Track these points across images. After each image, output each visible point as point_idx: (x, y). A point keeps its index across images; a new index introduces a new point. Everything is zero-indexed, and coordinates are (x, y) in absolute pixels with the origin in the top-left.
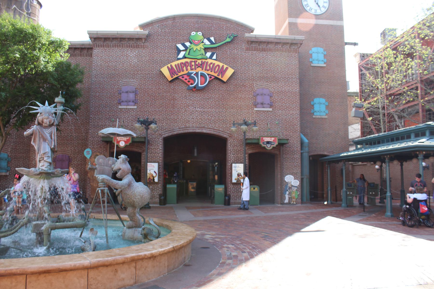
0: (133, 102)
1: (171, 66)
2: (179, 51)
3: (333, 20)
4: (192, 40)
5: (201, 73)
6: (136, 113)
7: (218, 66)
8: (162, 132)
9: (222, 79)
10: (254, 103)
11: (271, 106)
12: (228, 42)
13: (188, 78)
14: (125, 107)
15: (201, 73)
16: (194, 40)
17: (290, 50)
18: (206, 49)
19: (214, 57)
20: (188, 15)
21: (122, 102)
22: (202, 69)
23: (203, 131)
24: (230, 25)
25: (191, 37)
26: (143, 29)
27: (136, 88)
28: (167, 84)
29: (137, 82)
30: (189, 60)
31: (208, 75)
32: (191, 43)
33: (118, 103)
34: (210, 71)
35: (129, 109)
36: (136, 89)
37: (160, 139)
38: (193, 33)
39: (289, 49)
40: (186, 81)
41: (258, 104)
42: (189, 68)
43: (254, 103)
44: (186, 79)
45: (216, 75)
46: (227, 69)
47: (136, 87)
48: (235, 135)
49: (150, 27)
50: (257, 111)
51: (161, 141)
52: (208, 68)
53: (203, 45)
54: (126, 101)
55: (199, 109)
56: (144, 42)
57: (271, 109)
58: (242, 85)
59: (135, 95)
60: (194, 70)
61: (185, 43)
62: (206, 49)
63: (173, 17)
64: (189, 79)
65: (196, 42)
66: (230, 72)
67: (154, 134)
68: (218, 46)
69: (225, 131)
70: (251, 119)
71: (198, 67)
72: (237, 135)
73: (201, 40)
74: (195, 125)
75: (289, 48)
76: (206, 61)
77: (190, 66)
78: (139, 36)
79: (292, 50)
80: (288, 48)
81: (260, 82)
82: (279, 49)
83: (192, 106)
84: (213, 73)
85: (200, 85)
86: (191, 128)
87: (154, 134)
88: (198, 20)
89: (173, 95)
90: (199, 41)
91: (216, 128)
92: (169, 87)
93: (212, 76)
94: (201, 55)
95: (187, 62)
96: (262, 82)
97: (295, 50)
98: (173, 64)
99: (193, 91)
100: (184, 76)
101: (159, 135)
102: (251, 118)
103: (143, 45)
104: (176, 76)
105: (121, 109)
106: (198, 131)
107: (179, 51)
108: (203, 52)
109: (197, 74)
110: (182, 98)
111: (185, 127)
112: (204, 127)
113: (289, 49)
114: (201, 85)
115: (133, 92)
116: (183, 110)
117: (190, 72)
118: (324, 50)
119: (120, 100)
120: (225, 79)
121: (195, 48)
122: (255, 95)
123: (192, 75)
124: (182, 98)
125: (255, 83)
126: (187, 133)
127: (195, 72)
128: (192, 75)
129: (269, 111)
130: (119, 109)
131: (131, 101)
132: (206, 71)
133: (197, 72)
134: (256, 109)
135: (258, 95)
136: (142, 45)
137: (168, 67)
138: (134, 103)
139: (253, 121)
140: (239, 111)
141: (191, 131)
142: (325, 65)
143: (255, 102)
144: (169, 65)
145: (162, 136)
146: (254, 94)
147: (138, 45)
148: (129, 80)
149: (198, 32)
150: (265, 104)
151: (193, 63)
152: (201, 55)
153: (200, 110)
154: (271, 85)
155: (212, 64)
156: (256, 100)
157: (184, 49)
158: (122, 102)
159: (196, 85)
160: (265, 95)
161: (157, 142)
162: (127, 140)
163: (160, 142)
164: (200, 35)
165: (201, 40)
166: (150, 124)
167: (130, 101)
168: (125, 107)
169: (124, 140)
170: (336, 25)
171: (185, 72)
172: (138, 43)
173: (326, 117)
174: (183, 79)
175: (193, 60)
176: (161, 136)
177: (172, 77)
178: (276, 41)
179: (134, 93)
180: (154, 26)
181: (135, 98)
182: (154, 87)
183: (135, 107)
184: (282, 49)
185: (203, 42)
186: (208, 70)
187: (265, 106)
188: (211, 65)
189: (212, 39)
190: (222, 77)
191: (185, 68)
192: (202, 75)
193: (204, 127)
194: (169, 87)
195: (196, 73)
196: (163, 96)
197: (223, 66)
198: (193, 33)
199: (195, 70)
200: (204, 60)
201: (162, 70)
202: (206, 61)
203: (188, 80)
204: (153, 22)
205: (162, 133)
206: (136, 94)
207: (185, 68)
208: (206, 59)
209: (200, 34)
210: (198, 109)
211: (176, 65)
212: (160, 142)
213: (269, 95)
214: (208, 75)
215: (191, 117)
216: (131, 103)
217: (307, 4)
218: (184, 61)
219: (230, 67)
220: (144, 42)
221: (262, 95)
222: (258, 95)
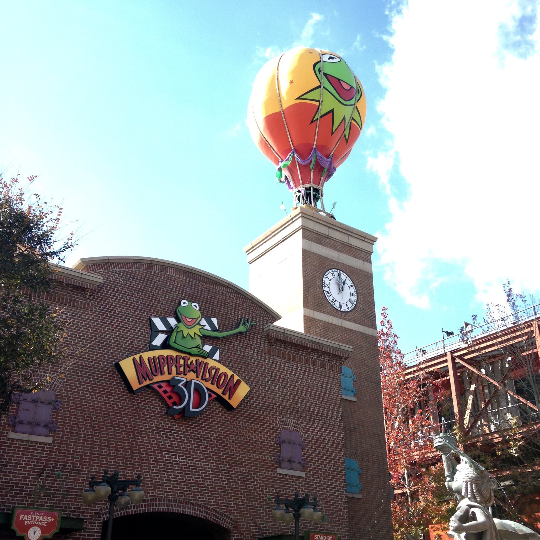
0: (46, 426)
1: (141, 357)
2: (155, 332)
3: (364, 325)
4: (181, 314)
5: (195, 383)
6: (49, 454)
7: (225, 374)
8: (102, 507)
9: (230, 401)
10: (276, 458)
11: (304, 468)
12: (241, 333)
13: (168, 389)
14: (25, 437)
15: (195, 383)
16: (185, 317)
17: (330, 365)
18: (205, 339)
19: (217, 356)
20: (177, 267)
21: (21, 422)
22: (197, 377)
23: (187, 510)
24: (242, 303)
25: (179, 308)
26: (88, 271)
27: (56, 395)
28: (124, 395)
29: (61, 380)
30: (174, 354)
31: (208, 389)
32: (178, 321)
33: (9, 425)
34: (210, 382)
35: (32, 442)
36: (56, 398)
37: (97, 524)
38: (184, 303)
39: (328, 364)
40: (165, 396)
41: (283, 460)
42: (174, 369)
43: (276, 458)
44: (165, 392)
45: (219, 392)
46: (238, 382)
47: (56, 393)
48: (244, 525)
49: (103, 271)
50: (281, 474)
51: (97, 529)
52: (207, 376)
53: (199, 329)
54: (29, 423)
55: (182, 459)
56: (87, 297)
57: (303, 474)
58: (259, 419)
59: (53, 412)
60: (182, 375)
61: (168, 318)
62: (205, 339)
63: (150, 262)
64: (172, 392)
65: (189, 320)
66: (243, 390)
67: (83, 512)
68: (224, 338)
69: (226, 514)
70: (271, 491)
71: (189, 371)
72: (247, 525)
73: (197, 318)
74: (171, 495)
75: (329, 362)
76: (205, 361)
77: (176, 366)
78: (82, 283)
79: (332, 365)
80: (327, 362)
81: (286, 418)
82: (314, 361)
83: (168, 451)
84: (214, 388)
85: (191, 409)
86: (163, 503)
87: (83, 512)
88: (191, 280)
89: (134, 421)
90: (193, 319)
91: (211, 505)
92: (128, 404)
93: (212, 394)
94: (196, 347)
95: (171, 357)
96: (288, 418)
97: (336, 366)
98: (146, 355)
99: (174, 419)
100: (163, 384)
101: (95, 513)
102: (271, 489)
103: (85, 303)
104: (148, 382)
105: (13, 440)
106: (177, 509)
107: (155, 332)
108: (199, 341)
109: (187, 384)
110: (151, 431)
111: (152, 498)
112: (188, 502)
113: (328, 364)
114: (193, 408)
115: (50, 404)
116: (152, 458)
117: (175, 378)
118: (354, 373)
119: (15, 418)
120: (235, 402)
121: (186, 331)
122: (278, 442)
123: (180, 385)
124: (151, 431)
125: (278, 418)
126: (156, 512)
127: (185, 380)
128: (180, 385)
129: (300, 477)
130: (9, 439)
131: (43, 424)
132: (204, 382)
133: (188, 380)
134: (279, 471)
135: (284, 442)
136: (81, 302)
137: (134, 360)
138: (48, 431)
139: (292, 499)
140: (252, 471)
141: (162, 508)
142: (354, 399)
143: (279, 456)
144: (137, 357)
145: (102, 519)
146: (277, 439)
147: (74, 300)
148: (42, 374)
149: (193, 302)
150: (294, 462)
151: (182, 362)
152: (196, 347)
153: (184, 462)
154: (302, 425)
155: (214, 369)
156: (280, 452)
157: (164, 329)
158: (21, 422)
159: (184, 408)
160: (294, 443)
161: (89, 532)
162: (48, 523)
163: (95, 532)
164: (195, 308)
165: (197, 318)
166: (300, 507)
167: (38, 424)
168: (25, 437)
169: (41, 523)
170: (367, 334)
171: (167, 377)
172: (74, 297)
173: (360, 496)
174: (160, 391)
175: (183, 355)
176: (99, 517)
177: (140, 383)
178: (312, 346)
179: (52, 407)
180: (111, 270)
181: (53, 418)
182: (97, 398)
183: (49, 440)
184: (319, 362)
185: (199, 324)
186: (206, 380)
187: (294, 465)
188: (213, 372)
189: (214, 320)
190: (230, 398)
191: (166, 368)
192: (198, 390)
193: (188, 502)
194: (128, 404)
195: (187, 382)
196: (114, 421)
197: (232, 376)
198: (184, 303)
199: (184, 376)
200: (201, 359)
201: (122, 363)
202: (205, 361)
203: (168, 394)
204: (110, 261)
205: (102, 511)
206: (55, 408)
207: (166, 368)
208: (205, 358)
209: (196, 306)
210: (179, 458)
211: (149, 359)
212: (95, 532)
213: (300, 445)
214: (208, 389)
215: (165, 477)
216: (40, 429)
217: (329, 292)
218: (166, 353)
219: (245, 382)
220: (88, 298)
221: (289, 443)
222: (284, 442)
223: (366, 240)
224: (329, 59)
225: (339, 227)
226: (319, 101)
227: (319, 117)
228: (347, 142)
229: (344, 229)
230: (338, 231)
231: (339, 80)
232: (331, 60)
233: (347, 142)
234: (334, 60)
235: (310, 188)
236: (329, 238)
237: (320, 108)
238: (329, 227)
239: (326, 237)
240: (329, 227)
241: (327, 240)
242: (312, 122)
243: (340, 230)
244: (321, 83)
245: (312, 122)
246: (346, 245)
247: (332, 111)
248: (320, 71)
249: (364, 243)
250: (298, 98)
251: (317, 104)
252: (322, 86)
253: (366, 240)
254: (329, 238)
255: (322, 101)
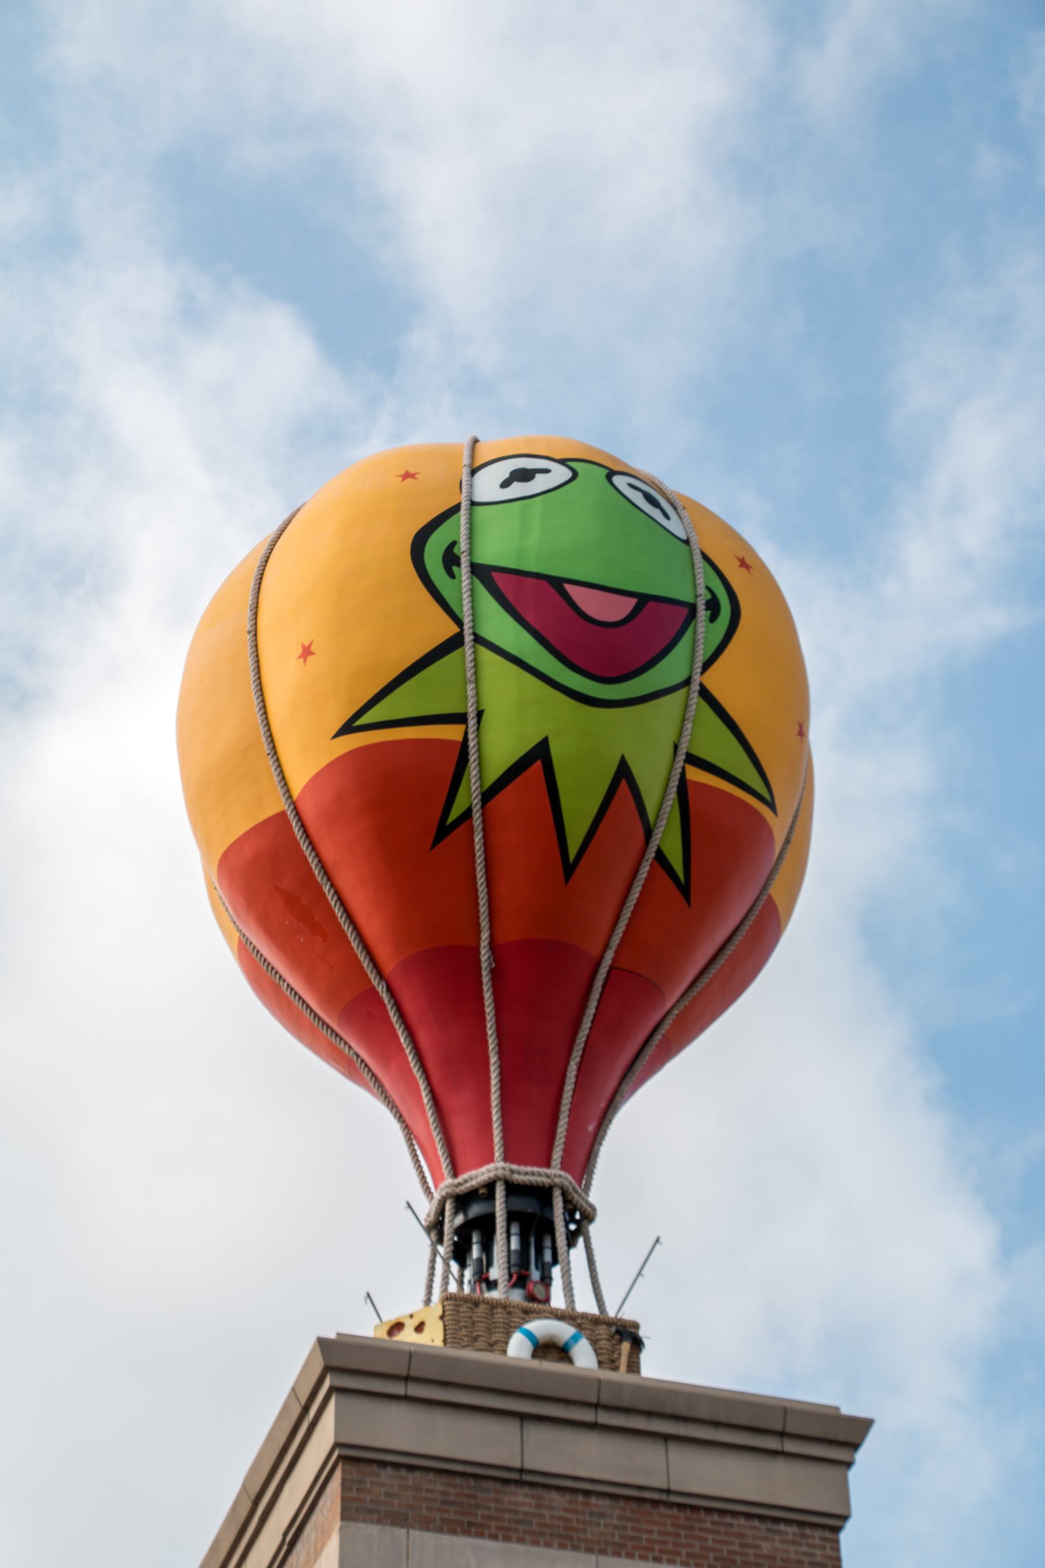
223: (790, 1446)
224: (505, 484)
225: (596, 1406)
226: (460, 718)
227: (476, 801)
228: (685, 890)
229: (627, 1411)
230: (593, 1426)
231: (557, 583)
232: (518, 489)
233: (685, 890)
234: (540, 483)
235: (490, 1186)
236: (532, 1485)
237: (473, 757)
238: (523, 1417)
239: (506, 1482)
240: (523, 1417)
241: (521, 1497)
242: (443, 831)
243: (604, 1418)
244: (459, 623)
245: (443, 831)
246: (656, 1503)
247: (541, 752)
248: (450, 559)
249: (780, 1468)
250: (348, 728)
251: (452, 733)
252: (468, 638)
253: (790, 1446)
254: (532, 1485)
255: (480, 715)
